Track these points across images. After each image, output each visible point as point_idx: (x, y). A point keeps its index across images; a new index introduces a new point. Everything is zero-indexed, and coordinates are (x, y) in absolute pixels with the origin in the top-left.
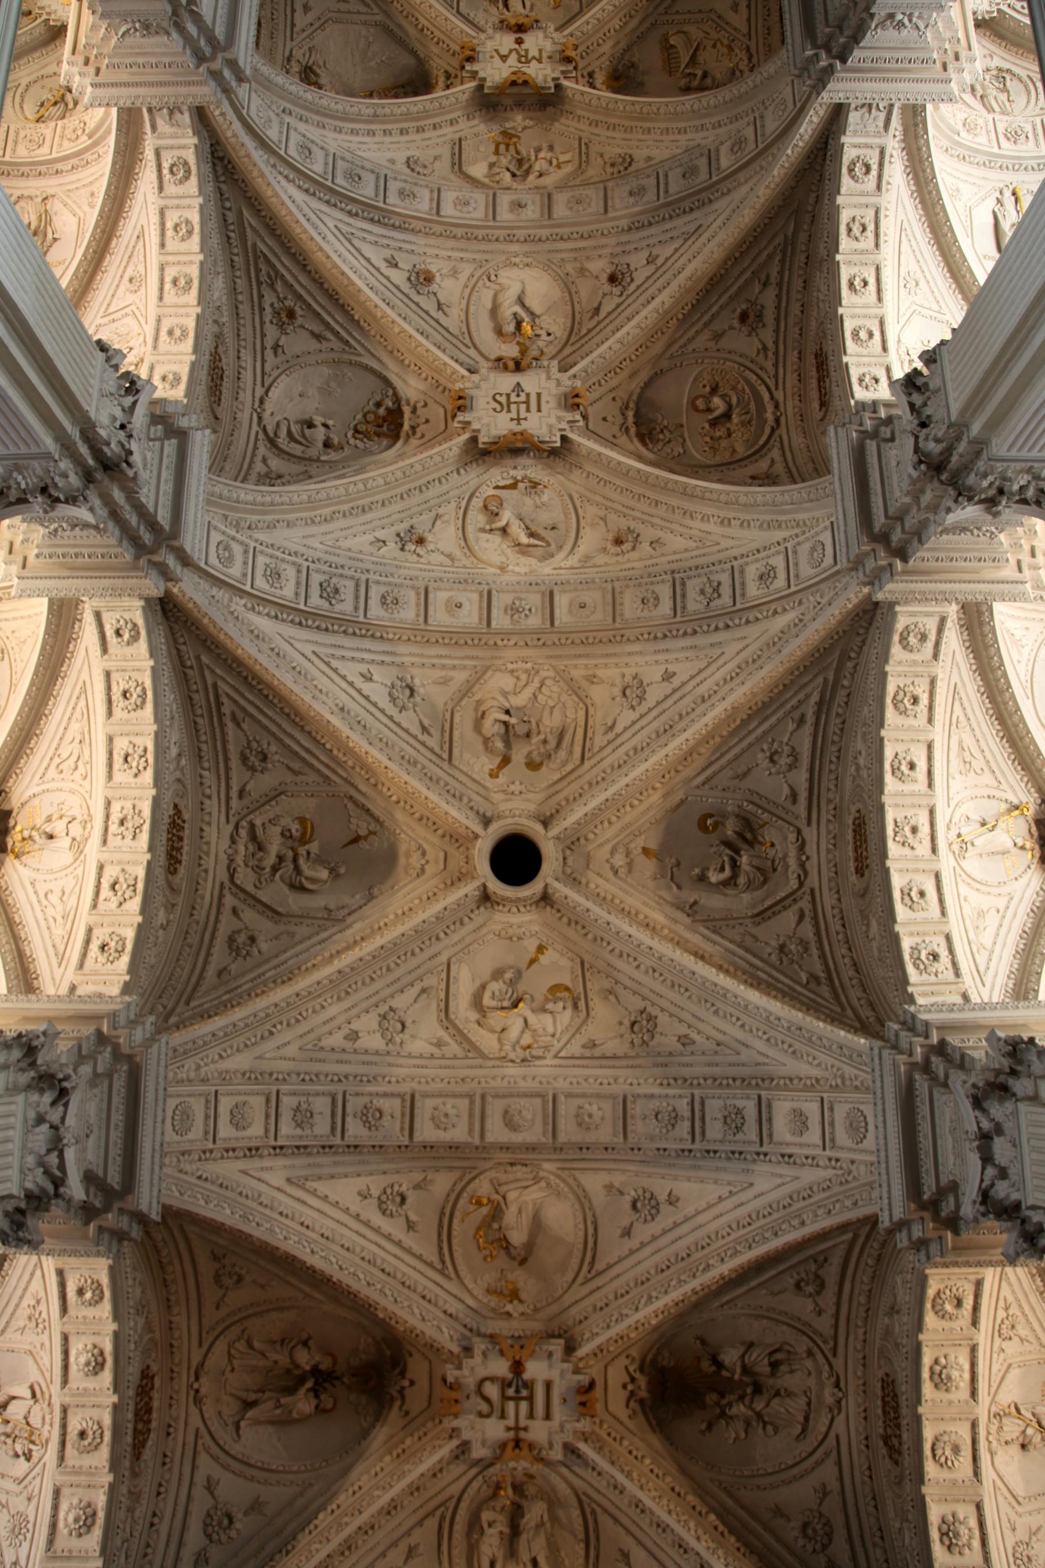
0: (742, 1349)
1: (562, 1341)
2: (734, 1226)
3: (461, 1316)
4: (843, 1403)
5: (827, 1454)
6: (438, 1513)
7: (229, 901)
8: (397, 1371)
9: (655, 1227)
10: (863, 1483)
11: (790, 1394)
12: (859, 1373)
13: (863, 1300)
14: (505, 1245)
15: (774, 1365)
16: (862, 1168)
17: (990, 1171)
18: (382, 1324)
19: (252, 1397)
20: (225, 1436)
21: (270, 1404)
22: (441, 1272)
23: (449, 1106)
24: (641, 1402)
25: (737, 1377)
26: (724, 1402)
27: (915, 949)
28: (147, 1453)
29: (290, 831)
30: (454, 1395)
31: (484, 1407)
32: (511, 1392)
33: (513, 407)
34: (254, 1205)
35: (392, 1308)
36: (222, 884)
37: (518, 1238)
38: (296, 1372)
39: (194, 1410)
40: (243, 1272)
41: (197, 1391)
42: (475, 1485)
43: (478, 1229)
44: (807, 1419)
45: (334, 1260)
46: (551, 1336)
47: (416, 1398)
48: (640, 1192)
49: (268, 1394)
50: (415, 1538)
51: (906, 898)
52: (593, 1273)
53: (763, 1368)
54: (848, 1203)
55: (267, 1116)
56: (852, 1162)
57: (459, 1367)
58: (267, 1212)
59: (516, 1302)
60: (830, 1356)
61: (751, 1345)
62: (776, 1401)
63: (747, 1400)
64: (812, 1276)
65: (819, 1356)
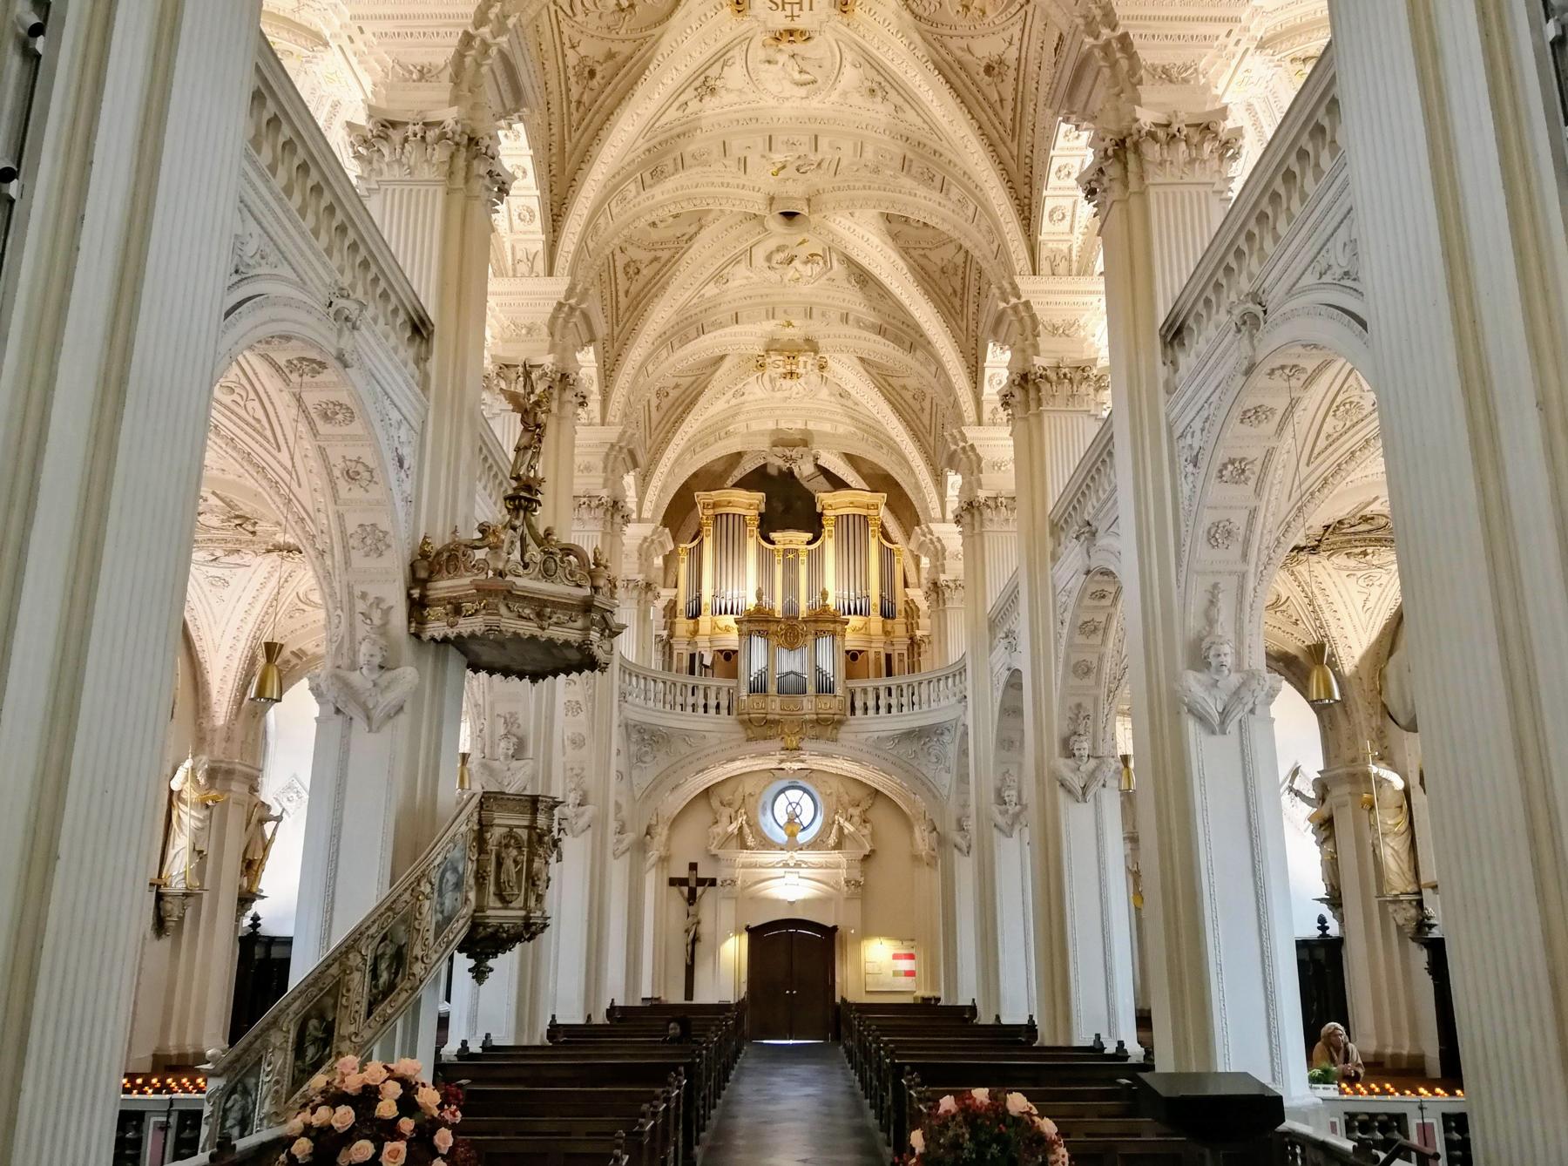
33: (788, 7)
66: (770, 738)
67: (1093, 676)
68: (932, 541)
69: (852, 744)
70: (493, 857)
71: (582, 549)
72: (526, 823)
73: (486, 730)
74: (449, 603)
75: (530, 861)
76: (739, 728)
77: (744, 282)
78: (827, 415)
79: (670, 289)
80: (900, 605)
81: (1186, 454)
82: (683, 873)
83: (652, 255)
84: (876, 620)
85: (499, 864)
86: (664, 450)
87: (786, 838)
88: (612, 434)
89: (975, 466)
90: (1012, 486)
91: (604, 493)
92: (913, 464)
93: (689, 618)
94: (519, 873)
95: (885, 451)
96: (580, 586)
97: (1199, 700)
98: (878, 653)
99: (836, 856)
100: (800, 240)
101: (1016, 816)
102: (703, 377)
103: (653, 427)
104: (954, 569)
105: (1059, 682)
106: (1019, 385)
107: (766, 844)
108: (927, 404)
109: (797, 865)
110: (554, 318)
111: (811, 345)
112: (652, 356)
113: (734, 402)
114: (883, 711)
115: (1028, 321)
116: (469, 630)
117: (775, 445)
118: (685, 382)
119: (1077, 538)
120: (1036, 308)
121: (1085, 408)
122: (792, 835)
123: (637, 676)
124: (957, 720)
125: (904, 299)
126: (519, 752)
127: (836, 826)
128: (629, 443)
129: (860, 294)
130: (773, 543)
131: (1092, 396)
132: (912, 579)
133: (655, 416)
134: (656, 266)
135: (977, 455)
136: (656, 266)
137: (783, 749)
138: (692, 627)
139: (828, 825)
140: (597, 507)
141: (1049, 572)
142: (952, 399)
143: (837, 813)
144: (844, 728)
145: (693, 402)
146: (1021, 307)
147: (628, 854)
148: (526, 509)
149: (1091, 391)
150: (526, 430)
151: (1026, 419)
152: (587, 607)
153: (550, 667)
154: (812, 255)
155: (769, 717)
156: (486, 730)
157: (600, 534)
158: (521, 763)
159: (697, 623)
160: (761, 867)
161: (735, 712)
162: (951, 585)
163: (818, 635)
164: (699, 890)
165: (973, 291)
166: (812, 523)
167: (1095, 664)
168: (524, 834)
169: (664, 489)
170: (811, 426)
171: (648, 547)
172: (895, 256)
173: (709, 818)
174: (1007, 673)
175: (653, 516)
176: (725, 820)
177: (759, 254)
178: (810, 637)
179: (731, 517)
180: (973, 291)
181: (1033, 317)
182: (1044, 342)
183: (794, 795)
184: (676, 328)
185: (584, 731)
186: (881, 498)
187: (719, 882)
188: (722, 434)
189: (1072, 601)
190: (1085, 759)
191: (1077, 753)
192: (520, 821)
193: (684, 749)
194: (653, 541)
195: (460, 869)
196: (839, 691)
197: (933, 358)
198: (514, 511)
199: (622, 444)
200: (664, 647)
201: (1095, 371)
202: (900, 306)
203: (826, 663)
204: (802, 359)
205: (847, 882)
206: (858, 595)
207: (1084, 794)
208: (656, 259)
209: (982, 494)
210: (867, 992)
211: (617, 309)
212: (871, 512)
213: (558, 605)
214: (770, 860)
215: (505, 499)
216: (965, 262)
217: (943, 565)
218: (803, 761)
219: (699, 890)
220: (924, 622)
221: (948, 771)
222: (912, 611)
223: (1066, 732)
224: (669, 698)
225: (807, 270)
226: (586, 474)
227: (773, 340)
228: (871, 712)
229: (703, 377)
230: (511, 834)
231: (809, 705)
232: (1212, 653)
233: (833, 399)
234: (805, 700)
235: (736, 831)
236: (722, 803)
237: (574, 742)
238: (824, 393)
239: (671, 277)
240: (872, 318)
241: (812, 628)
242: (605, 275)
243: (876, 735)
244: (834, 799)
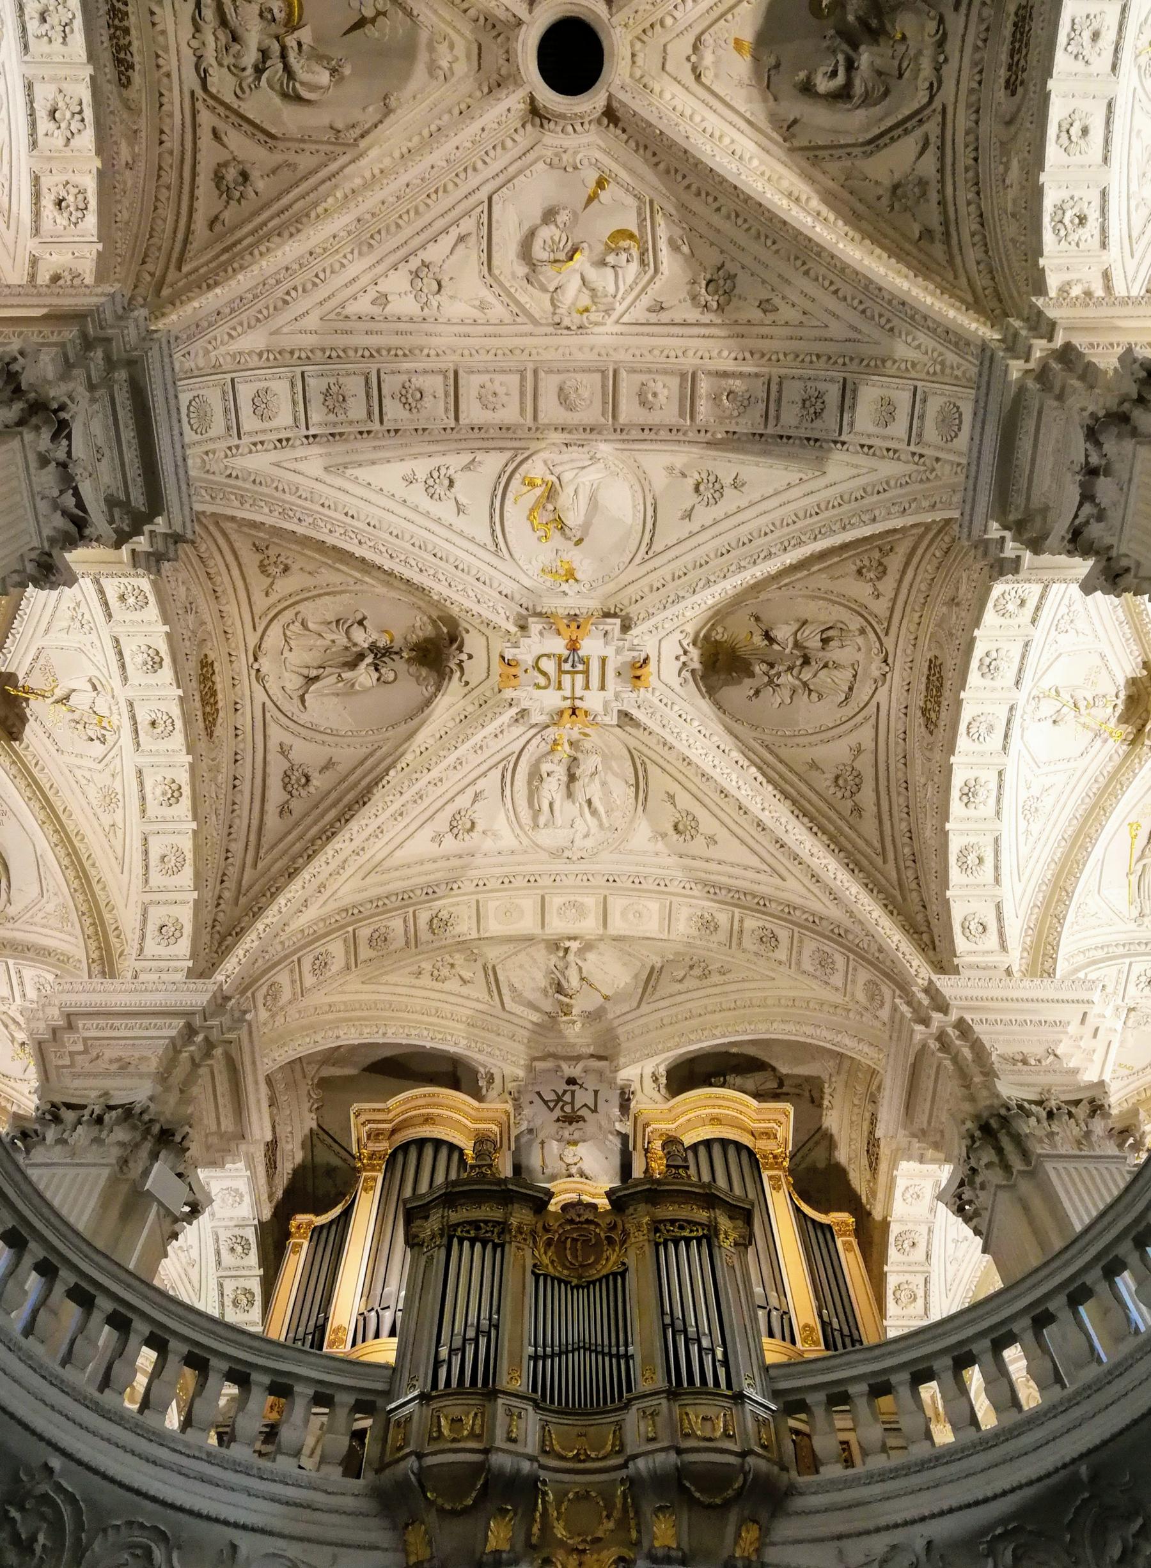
0: (796, 626)
1: (618, 621)
2: (801, 515)
3: (517, 597)
4: (889, 676)
5: (866, 719)
6: (501, 766)
7: (206, 118)
8: (455, 646)
9: (717, 511)
10: (897, 743)
11: (837, 666)
12: (909, 652)
13: (923, 587)
14: (561, 525)
15: (825, 641)
16: (948, 467)
17: (1088, 509)
18: (436, 605)
19: (314, 673)
20: (292, 708)
21: (333, 679)
22: (496, 554)
23: (497, 383)
24: (693, 671)
25: (788, 651)
26: (773, 672)
27: (1060, 208)
28: (218, 731)
29: (271, 10)
30: (513, 671)
31: (542, 681)
32: (567, 667)
34: (293, 499)
35: (446, 592)
36: (193, 93)
37: (573, 519)
38: (354, 649)
39: (257, 687)
40: (289, 562)
41: (258, 670)
42: (534, 742)
43: (532, 510)
44: (851, 689)
45: (383, 549)
46: (607, 615)
47: (475, 670)
48: (704, 475)
49: (328, 670)
50: (481, 784)
51: (1064, 135)
52: (651, 554)
53: (814, 643)
54: (925, 504)
55: (294, 403)
56: (938, 460)
57: (516, 645)
58: (308, 504)
59: (571, 581)
60: (882, 635)
61: (805, 622)
62: (823, 674)
63: (795, 672)
64: (875, 564)
65: (872, 635)
76: (376, 1532)
108: (867, 797)
118: (346, 755)
133: (272, 820)
145: (362, 800)
155: (499, 1460)
165: (969, 225)
180: (969, 225)
216: (941, 171)
233: (660, 846)
243: (918, 1537)
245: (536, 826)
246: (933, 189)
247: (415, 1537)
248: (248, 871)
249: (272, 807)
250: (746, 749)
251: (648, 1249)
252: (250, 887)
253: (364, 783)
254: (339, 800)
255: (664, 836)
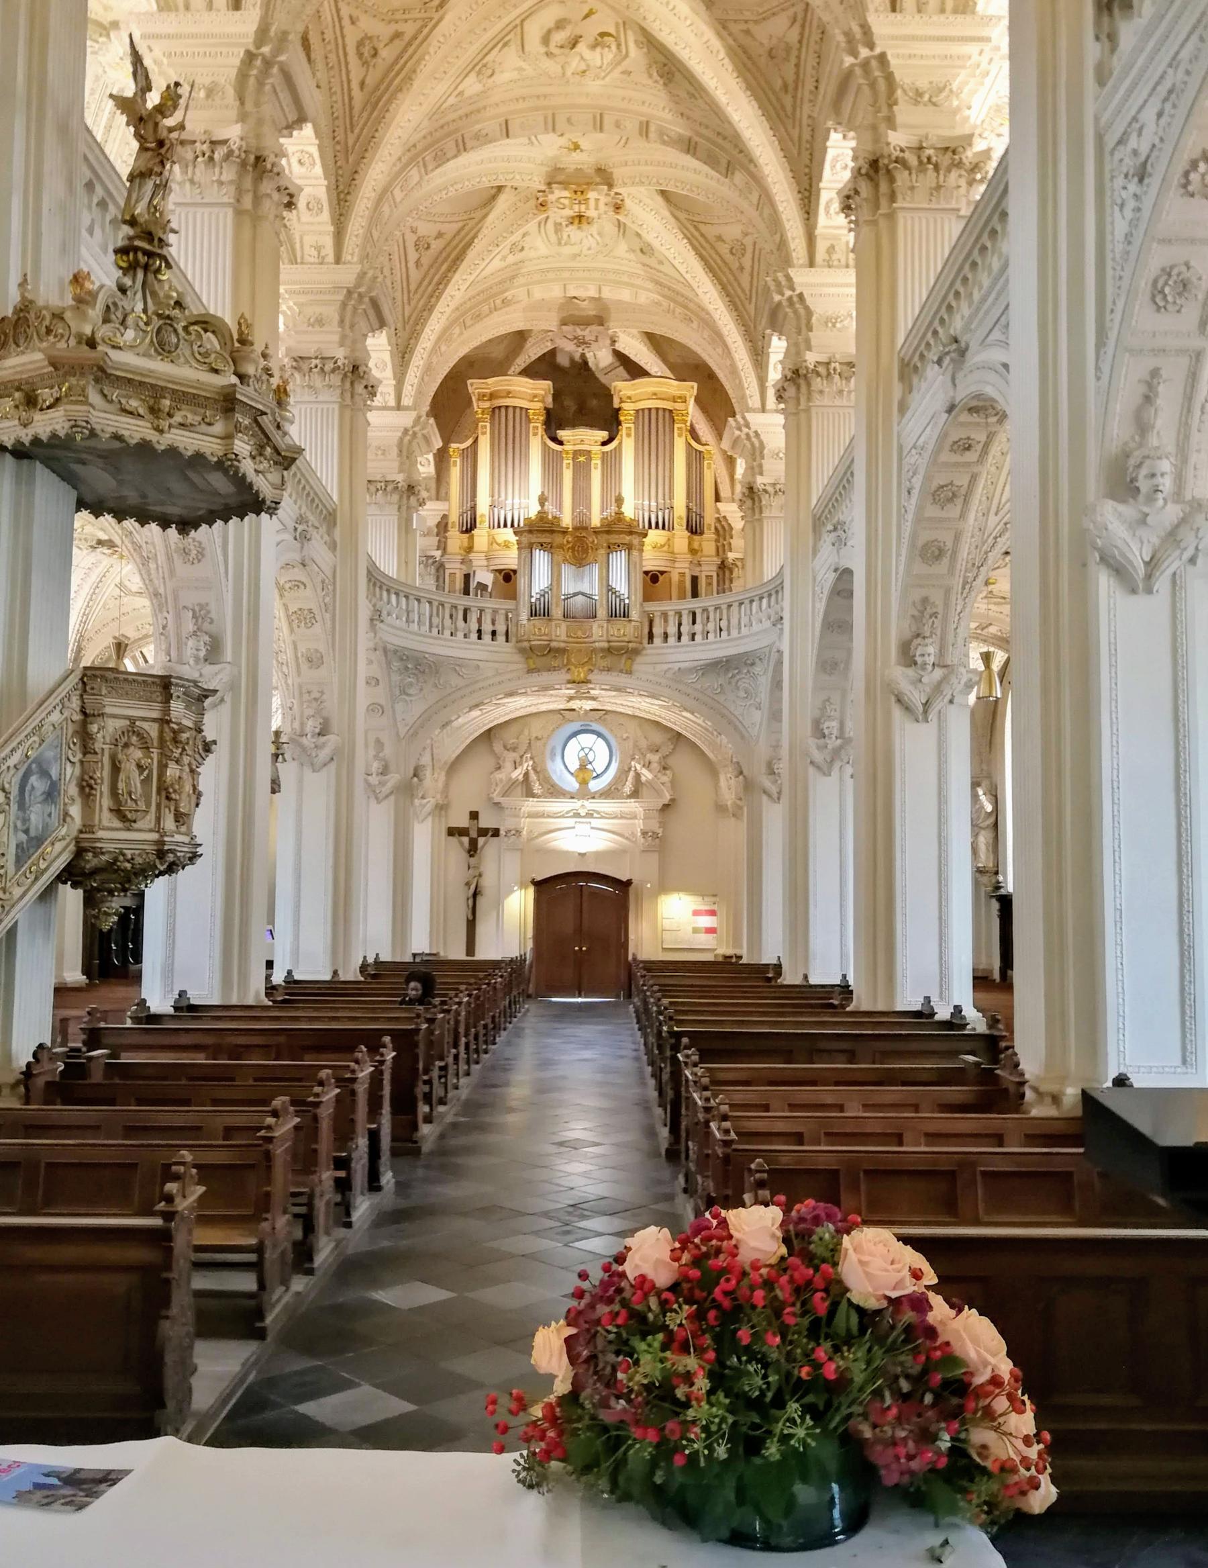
66: (555, 669)
67: (945, 561)
68: (748, 435)
69: (651, 678)
70: (106, 760)
71: (222, 320)
72: (155, 715)
73: (171, 626)
74: (18, 389)
75: (163, 767)
76: (518, 658)
77: (515, 75)
78: (625, 279)
79: (417, 83)
80: (709, 519)
81: (1130, 164)
82: (463, 822)
83: (394, 27)
84: (681, 537)
85: (116, 769)
86: (426, 320)
87: (577, 786)
88: (347, 275)
89: (804, 322)
90: (852, 349)
91: (340, 354)
92: (729, 340)
93: (462, 532)
94: (146, 781)
95: (695, 325)
96: (216, 371)
97: (1119, 543)
98: (682, 574)
99: (633, 806)
100: (586, 11)
101: (837, 752)
102: (472, 223)
103: (413, 287)
104: (774, 471)
105: (902, 568)
106: (867, 174)
107: (555, 792)
108: (747, 261)
109: (589, 815)
110: (242, 76)
111: (604, 176)
112: (398, 175)
113: (511, 259)
114: (685, 638)
115: (882, 85)
116: (49, 429)
117: (564, 322)
118: (450, 229)
119: (939, 362)
120: (893, 61)
121: (953, 205)
122: (584, 783)
123: (397, 594)
124: (770, 646)
125: (721, 97)
126: (213, 652)
127: (632, 774)
128: (370, 289)
129: (663, 94)
130: (561, 443)
131: (963, 190)
132: (725, 491)
134: (398, 45)
135: (807, 308)
136: (398, 45)
137: (569, 682)
138: (466, 544)
139: (623, 772)
140: (333, 371)
141: (895, 428)
142: (777, 238)
143: (633, 759)
144: (639, 659)
145: (460, 258)
146: (874, 63)
147: (392, 798)
148: (146, 268)
149: (963, 182)
150: (143, 149)
151: (874, 223)
152: (228, 403)
153: (203, 507)
154: (603, 35)
155: (554, 644)
156: (171, 626)
157: (336, 407)
158: (216, 668)
159: (471, 538)
160: (549, 816)
161: (513, 639)
162: (770, 489)
163: (610, 548)
164: (481, 841)
165: (809, 85)
166: (610, 421)
167: (949, 545)
168: (153, 730)
169: (428, 369)
170: (607, 294)
171: (410, 442)
172: (709, 34)
173: (490, 762)
174: (832, 576)
175: (415, 403)
176: (508, 765)
177: (534, 30)
178: (602, 551)
179: (511, 411)
180: (809, 85)
181: (889, 78)
182: (903, 112)
183: (586, 739)
184: (429, 139)
185: (322, 648)
186: (690, 389)
187: (502, 832)
188: (498, 302)
189: (923, 463)
190: (930, 668)
191: (919, 660)
192: (145, 711)
193: (455, 681)
194: (415, 434)
195: (54, 773)
196: (634, 614)
197: (756, 179)
198: (130, 269)
199: (362, 290)
200: (437, 570)
201: (969, 153)
202: (715, 109)
203: (620, 583)
204: (592, 195)
205: (644, 833)
206: (661, 506)
207: (925, 712)
208: (397, 35)
209: (811, 358)
210: (664, 949)
211: (351, 108)
212: (679, 406)
213: (184, 398)
214: (559, 810)
215: (116, 251)
216: (800, 42)
217: (761, 466)
218: (594, 699)
219: (481, 841)
220: (737, 542)
221: (759, 708)
222: (723, 530)
223: (908, 634)
224: (436, 621)
225: (596, 58)
226: (317, 328)
227: (558, 170)
228: (672, 640)
229: (472, 223)
230: (132, 728)
231: (599, 632)
232: (1144, 472)
233: (632, 256)
234: (595, 626)
235: (521, 778)
236: (505, 747)
237: (310, 661)
238: (622, 248)
239: (418, 62)
240: (679, 128)
241: (603, 540)
242: (332, 57)
243: (676, 666)
244: (631, 744)
245: (560, 244)
246: (794, 53)
247: (531, 661)
248: (406, 307)
249: (411, 265)
250: (682, 227)
251: (605, 556)
252: (409, 318)
253: (461, 246)
254: (449, 256)
255: (634, 251)
